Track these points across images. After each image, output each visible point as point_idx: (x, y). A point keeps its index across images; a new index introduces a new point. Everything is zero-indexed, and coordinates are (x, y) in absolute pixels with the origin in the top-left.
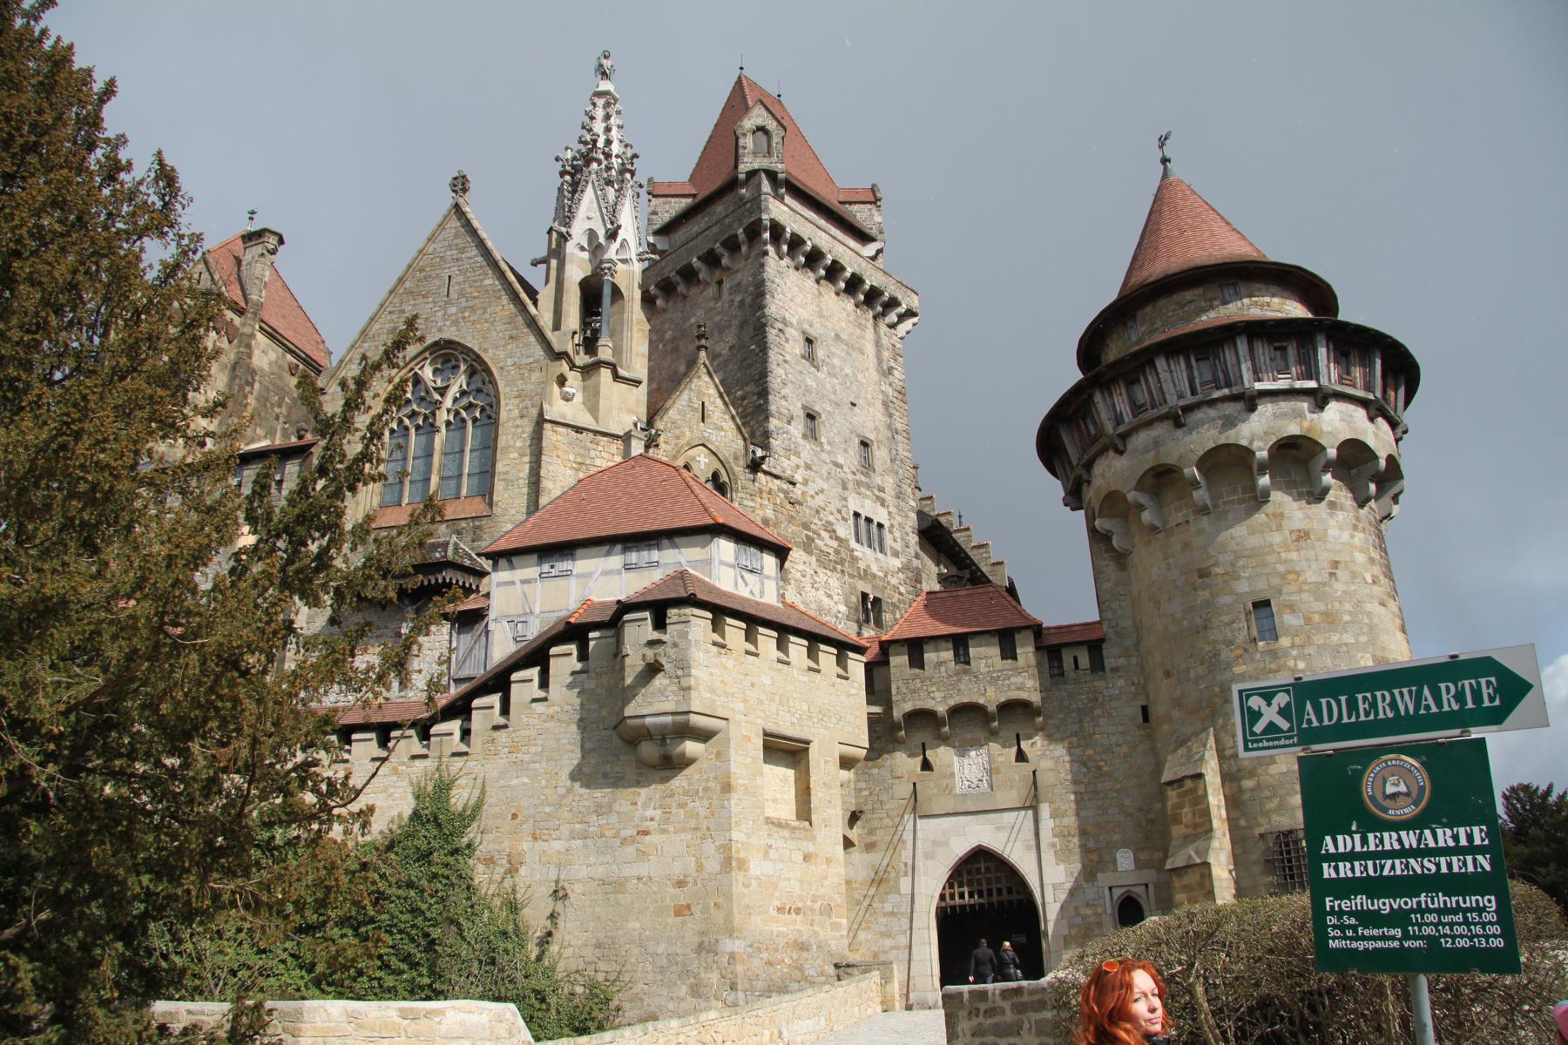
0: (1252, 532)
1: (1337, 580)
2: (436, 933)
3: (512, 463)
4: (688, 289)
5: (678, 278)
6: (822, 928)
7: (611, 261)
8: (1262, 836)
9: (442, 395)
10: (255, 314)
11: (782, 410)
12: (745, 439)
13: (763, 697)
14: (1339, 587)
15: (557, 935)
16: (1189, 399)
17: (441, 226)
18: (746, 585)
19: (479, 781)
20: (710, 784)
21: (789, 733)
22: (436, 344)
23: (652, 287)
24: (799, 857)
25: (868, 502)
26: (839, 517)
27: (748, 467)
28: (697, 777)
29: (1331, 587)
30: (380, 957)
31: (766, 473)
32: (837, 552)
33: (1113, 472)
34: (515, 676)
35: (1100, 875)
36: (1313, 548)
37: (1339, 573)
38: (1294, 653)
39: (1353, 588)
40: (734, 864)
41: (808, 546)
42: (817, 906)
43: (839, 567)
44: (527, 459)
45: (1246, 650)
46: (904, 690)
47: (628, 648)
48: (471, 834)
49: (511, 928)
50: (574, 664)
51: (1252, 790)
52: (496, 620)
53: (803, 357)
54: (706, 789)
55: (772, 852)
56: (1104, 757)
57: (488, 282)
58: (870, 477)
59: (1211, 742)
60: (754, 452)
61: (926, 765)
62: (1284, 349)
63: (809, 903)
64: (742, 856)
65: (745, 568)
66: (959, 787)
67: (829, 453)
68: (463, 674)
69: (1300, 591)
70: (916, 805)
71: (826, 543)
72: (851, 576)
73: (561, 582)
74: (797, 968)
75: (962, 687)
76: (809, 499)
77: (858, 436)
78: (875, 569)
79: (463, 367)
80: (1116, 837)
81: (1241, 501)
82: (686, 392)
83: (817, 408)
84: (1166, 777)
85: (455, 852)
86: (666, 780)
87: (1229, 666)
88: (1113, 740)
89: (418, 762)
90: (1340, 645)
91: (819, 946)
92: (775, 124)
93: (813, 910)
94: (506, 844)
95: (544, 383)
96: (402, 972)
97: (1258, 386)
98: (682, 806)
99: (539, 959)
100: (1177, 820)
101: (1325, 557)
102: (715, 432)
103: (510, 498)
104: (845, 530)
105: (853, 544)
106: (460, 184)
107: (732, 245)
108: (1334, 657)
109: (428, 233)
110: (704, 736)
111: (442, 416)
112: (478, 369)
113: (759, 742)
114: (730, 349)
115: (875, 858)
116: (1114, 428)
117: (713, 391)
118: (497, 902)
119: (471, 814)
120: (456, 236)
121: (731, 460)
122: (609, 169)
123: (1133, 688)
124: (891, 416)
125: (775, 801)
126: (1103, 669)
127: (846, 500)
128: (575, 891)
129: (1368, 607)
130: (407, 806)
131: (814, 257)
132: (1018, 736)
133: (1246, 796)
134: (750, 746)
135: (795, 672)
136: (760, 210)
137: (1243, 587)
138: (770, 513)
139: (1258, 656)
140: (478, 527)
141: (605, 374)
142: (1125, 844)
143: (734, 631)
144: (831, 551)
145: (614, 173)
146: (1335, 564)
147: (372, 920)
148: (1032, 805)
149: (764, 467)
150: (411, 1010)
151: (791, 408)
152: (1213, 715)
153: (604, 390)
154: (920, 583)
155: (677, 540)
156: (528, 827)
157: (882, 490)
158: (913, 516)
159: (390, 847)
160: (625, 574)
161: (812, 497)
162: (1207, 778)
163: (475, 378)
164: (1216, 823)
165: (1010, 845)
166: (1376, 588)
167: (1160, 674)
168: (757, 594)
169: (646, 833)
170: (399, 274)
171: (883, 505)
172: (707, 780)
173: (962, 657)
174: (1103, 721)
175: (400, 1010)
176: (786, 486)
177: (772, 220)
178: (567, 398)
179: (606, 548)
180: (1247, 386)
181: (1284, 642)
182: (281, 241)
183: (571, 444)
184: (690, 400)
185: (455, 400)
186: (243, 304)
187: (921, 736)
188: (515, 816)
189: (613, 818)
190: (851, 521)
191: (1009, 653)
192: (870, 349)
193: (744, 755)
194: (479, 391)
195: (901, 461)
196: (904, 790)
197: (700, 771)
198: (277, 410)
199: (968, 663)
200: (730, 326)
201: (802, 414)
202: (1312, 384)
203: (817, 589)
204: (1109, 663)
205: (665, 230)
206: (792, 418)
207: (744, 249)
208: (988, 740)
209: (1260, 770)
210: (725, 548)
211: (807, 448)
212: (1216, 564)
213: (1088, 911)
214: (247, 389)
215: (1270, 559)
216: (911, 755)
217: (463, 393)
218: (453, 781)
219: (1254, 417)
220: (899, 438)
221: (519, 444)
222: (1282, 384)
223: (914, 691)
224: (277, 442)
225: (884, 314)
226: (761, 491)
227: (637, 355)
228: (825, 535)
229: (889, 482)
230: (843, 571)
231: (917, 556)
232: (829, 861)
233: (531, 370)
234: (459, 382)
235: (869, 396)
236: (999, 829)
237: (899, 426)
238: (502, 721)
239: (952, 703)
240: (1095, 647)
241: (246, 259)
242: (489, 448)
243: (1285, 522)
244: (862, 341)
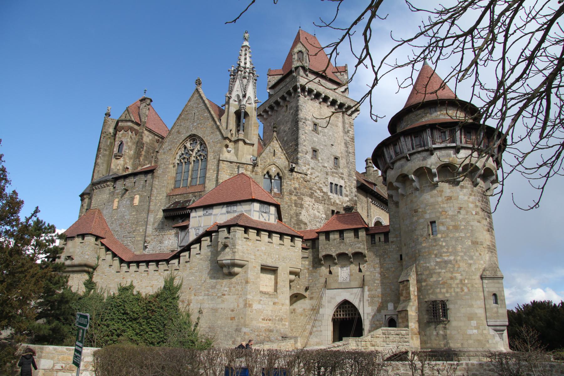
0: (432, 197)
1: (460, 214)
2: (166, 322)
3: (211, 174)
4: (278, 108)
5: (274, 105)
6: (279, 325)
7: (244, 105)
8: (426, 302)
9: (192, 152)
10: (143, 125)
11: (304, 150)
12: (289, 161)
13: (262, 254)
14: (461, 216)
15: (199, 324)
16: (412, 151)
17: (192, 96)
18: (263, 217)
19: (181, 278)
20: (243, 281)
21: (270, 265)
22: (190, 135)
23: (267, 108)
25: (336, 179)
26: (324, 185)
27: (289, 171)
28: (239, 278)
29: (458, 216)
30: (152, 328)
31: (296, 172)
32: (323, 197)
33: (392, 174)
34: (192, 247)
35: (382, 311)
36: (453, 203)
37: (461, 211)
38: (442, 240)
39: (466, 216)
40: (247, 305)
41: (311, 196)
42: (277, 319)
43: (323, 202)
44: (216, 172)
45: (426, 238)
46: (323, 248)
47: (219, 240)
48: (179, 293)
49: (187, 322)
50: (208, 242)
51: (425, 286)
52: (191, 228)
53: (313, 131)
54: (241, 282)
55: (261, 302)
56: (386, 272)
57: (205, 114)
58: (338, 170)
59: (414, 269)
60: (292, 165)
61: (330, 272)
62: (444, 132)
63: (274, 318)
64: (250, 303)
65: (263, 212)
66: (340, 280)
67: (321, 163)
68: (182, 245)
69: (446, 218)
70: (326, 285)
71: (319, 194)
72: (327, 204)
73: (209, 217)
74: (268, 337)
75: (341, 247)
76: (313, 180)
77: (334, 156)
78: (338, 201)
79: (198, 142)
80: (388, 299)
81: (429, 186)
82: (269, 147)
83: (317, 148)
84: (400, 280)
85: (174, 298)
86: (231, 279)
87: (421, 243)
88: (390, 266)
89: (166, 272)
90: (459, 237)
91: (277, 331)
92: (305, 49)
93: (275, 319)
94: (187, 297)
95: (221, 148)
96: (157, 333)
97: (434, 146)
98: (234, 287)
99: (194, 330)
100: (402, 295)
101: (457, 206)
102: (278, 160)
103: (210, 185)
104: (326, 189)
105: (329, 194)
106: (198, 83)
107: (289, 93)
108: (456, 242)
109: (188, 99)
110: (241, 266)
111: (193, 159)
112: (203, 143)
113: (259, 268)
114: (289, 129)
115: (314, 302)
116: (390, 161)
117: (278, 146)
118: (184, 313)
119: (179, 288)
120: (197, 99)
121: (283, 169)
122: (245, 73)
123: (398, 248)
124: (347, 147)
125: (266, 286)
126: (388, 242)
127: (327, 179)
128: (205, 311)
129: (472, 223)
130: (162, 285)
131: (318, 95)
132: (359, 263)
133: (423, 288)
134: (256, 269)
135: (275, 246)
136: (297, 81)
137: (427, 216)
138: (297, 186)
139: (430, 240)
140: (201, 195)
141: (241, 143)
142: (391, 301)
143: (252, 233)
144: (320, 197)
145: (247, 74)
146: (460, 208)
147: (151, 318)
148: (362, 286)
149: (295, 170)
150: (69, 348)
151: (307, 149)
152: (416, 260)
153: (240, 149)
154: (356, 205)
155: (242, 204)
156: (193, 292)
157: (342, 174)
158: (355, 182)
159: (157, 297)
160: (227, 215)
161: (314, 179)
162: (410, 282)
163: (202, 146)
164: (412, 297)
165: (355, 300)
166: (477, 217)
167: (403, 245)
168: (267, 219)
169: (224, 295)
170: (180, 113)
171: (342, 179)
172: (242, 280)
174: (387, 259)
175: (66, 348)
176: (303, 176)
177: (301, 85)
178: (229, 152)
179: (222, 206)
180: (430, 146)
181: (439, 236)
182: (151, 101)
183: (228, 167)
184: (270, 150)
185: (196, 153)
186: (140, 123)
187: (329, 263)
188: (190, 289)
189: (216, 290)
190: (329, 186)
191: (357, 236)
192: (340, 125)
193: (253, 272)
194: (203, 150)
195: (351, 163)
196: (323, 280)
197: (240, 277)
198: (152, 155)
199: (343, 239)
200: (289, 121)
201: (311, 150)
202: (454, 145)
203: (314, 210)
204: (391, 239)
205: (273, 87)
206: (307, 152)
207: (293, 95)
208: (350, 264)
209: (428, 280)
210: (256, 206)
211: (313, 163)
212: (420, 208)
213: (377, 323)
214: (141, 149)
215: (437, 207)
216: (326, 268)
217: (199, 151)
218: (174, 278)
219: (433, 157)
220: (350, 155)
221: (213, 168)
222: (443, 145)
223: (326, 248)
224: (153, 165)
225: (346, 111)
226: (294, 178)
227: (254, 135)
228: (318, 191)
229: (345, 171)
230: (325, 203)
231: (356, 196)
232: (283, 305)
233: (217, 143)
234: (198, 147)
235: (339, 141)
236: (351, 294)
237: (351, 151)
238: (188, 260)
239: (337, 252)
240: (386, 234)
241: (141, 107)
242: (205, 169)
243: (443, 194)
244: (337, 122)
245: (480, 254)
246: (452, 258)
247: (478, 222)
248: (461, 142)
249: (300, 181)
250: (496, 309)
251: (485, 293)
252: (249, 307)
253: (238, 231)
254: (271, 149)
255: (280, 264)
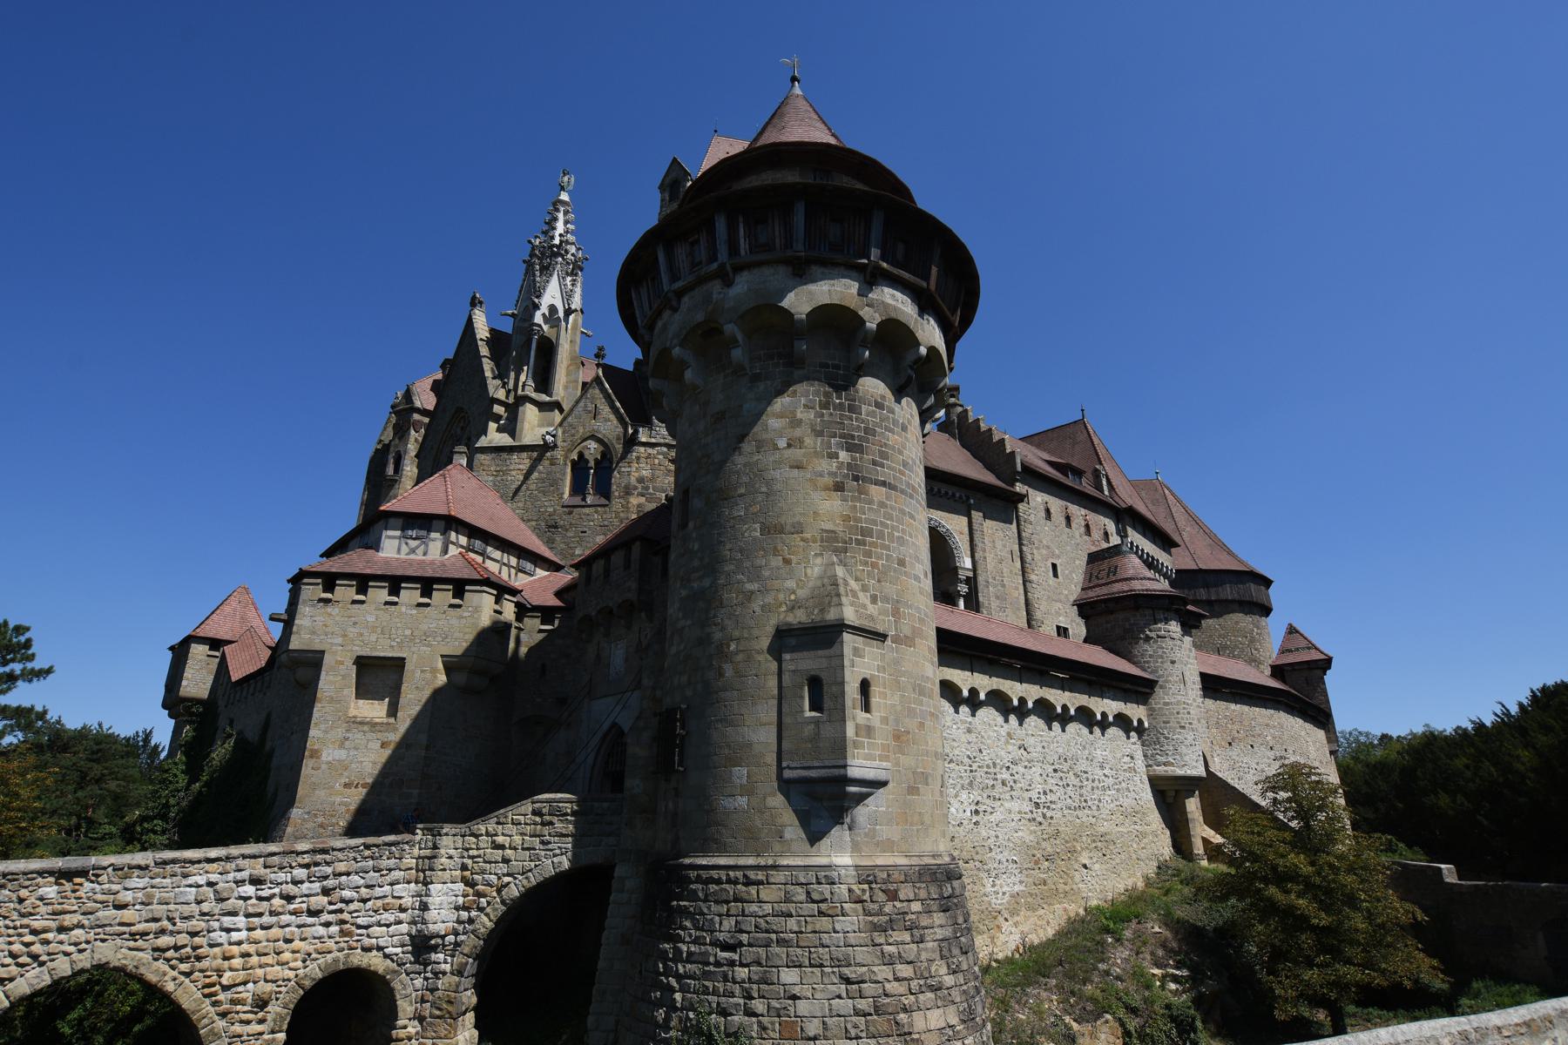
24: (379, 745)
55: (347, 743)
135: (403, 609)
173: (607, 572)
184: (586, 406)
245: (787, 562)
246: (707, 582)
247: (791, 467)
248: (733, 249)
249: (657, 461)
250: (813, 726)
251: (786, 678)
252: (311, 757)
253: (303, 587)
254: (589, 405)
255: (413, 649)
